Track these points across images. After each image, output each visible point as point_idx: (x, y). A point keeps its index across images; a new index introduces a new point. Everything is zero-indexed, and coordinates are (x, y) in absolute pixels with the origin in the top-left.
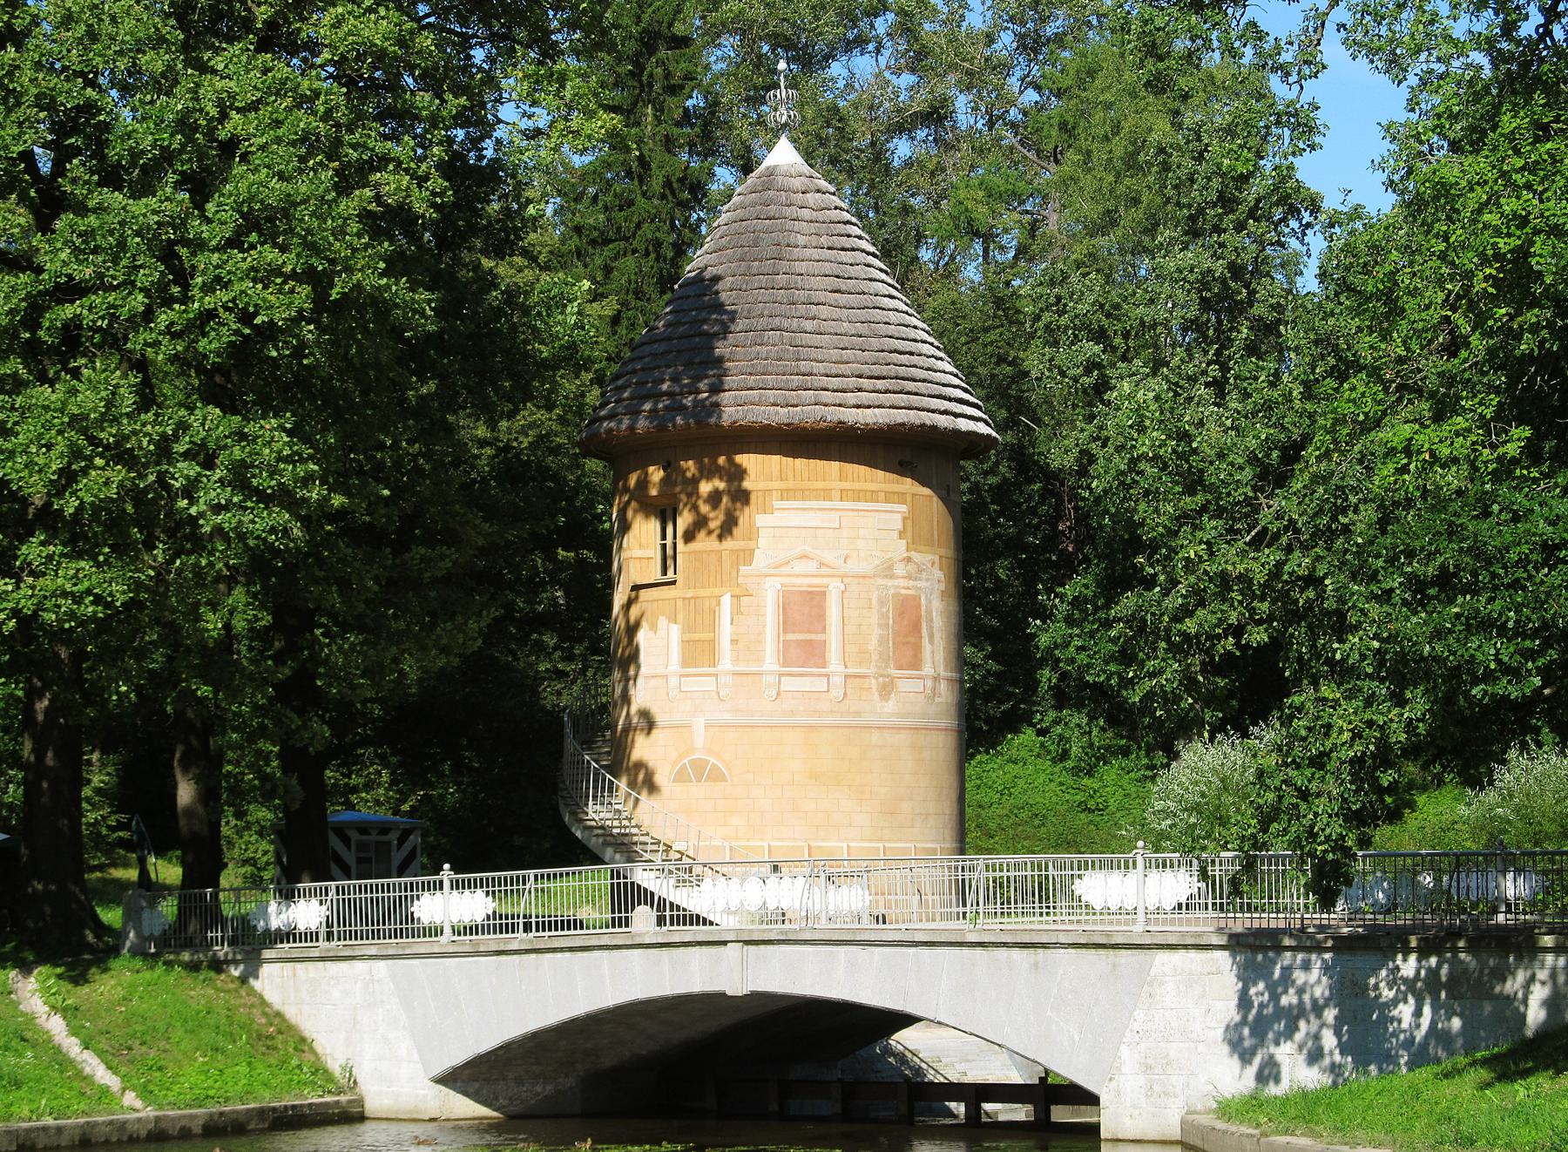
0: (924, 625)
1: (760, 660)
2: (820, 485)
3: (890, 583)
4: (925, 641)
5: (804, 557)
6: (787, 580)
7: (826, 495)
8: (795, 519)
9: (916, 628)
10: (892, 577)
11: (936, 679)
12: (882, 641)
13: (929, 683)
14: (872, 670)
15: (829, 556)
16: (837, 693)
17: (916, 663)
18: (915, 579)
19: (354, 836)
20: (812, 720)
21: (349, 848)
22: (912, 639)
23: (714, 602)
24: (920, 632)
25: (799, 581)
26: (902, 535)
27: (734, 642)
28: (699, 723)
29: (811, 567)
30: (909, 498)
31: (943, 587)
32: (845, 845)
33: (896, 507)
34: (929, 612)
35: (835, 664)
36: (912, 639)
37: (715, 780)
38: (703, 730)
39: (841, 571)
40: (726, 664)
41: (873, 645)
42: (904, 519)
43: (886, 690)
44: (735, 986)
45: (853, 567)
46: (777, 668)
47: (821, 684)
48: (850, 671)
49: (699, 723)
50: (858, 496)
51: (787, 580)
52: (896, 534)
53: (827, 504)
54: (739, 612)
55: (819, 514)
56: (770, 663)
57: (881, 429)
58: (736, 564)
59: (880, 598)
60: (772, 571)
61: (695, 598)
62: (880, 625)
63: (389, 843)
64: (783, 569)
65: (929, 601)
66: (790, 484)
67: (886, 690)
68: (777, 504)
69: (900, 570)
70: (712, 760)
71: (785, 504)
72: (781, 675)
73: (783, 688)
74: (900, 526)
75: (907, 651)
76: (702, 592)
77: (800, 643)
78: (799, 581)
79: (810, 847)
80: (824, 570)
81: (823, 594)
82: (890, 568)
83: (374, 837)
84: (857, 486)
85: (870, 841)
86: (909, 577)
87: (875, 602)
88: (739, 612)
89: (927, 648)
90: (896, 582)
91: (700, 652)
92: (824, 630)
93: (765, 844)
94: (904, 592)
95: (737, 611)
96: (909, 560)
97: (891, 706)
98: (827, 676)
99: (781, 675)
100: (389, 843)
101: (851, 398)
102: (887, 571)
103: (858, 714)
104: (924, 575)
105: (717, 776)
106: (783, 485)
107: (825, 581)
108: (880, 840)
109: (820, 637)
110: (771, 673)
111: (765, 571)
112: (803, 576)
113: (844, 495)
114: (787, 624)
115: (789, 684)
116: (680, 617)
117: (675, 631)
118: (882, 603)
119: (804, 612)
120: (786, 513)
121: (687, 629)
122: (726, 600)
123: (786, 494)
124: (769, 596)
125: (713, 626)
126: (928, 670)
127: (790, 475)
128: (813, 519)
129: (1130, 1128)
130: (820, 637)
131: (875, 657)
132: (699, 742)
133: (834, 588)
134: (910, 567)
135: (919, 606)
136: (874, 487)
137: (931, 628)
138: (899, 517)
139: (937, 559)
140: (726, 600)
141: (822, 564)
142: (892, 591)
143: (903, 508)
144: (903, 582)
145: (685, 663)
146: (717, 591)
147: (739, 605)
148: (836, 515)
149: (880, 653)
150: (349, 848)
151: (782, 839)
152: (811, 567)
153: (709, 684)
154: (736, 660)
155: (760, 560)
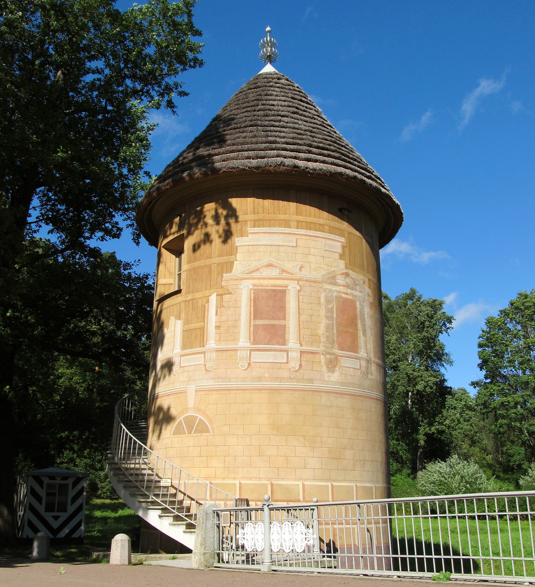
0: (359, 321)
1: (236, 340)
2: (282, 217)
3: (334, 288)
4: (360, 334)
6: (256, 282)
7: (287, 224)
8: (265, 239)
9: (353, 323)
10: (335, 284)
11: (368, 361)
12: (328, 328)
13: (364, 363)
14: (321, 348)
15: (288, 266)
16: (294, 364)
17: (354, 347)
19: (46, 481)
20: (276, 384)
21: (42, 487)
22: (351, 330)
23: (205, 300)
24: (356, 326)
25: (266, 282)
26: (342, 257)
27: (218, 327)
28: (191, 389)
29: (275, 273)
30: (346, 235)
31: (371, 300)
32: (300, 483)
33: (337, 238)
35: (292, 343)
36: (351, 330)
37: (201, 432)
38: (194, 393)
39: (298, 276)
40: (211, 344)
41: (321, 330)
42: (343, 247)
43: (332, 364)
45: (306, 274)
46: (248, 345)
47: (281, 358)
48: (305, 348)
49: (191, 389)
50: (309, 226)
51: (256, 282)
52: (337, 256)
53: (287, 230)
54: (222, 306)
55: (281, 236)
56: (243, 341)
57: (325, 175)
58: (220, 274)
59: (326, 297)
60: (246, 276)
61: (193, 300)
62: (327, 317)
63: (67, 485)
64: (254, 274)
65: (362, 307)
66: (261, 216)
67: (332, 364)
68: (250, 230)
69: (341, 280)
70: (200, 417)
71: (256, 230)
72: (251, 350)
73: (253, 360)
74: (340, 250)
76: (198, 295)
77: (265, 327)
78: (266, 282)
79: (272, 485)
80: (285, 275)
82: (334, 278)
83: (58, 481)
84: (309, 219)
85: (321, 480)
86: (347, 286)
87: (323, 300)
88: (222, 306)
89: (361, 339)
91: (194, 338)
92: (284, 318)
93: (237, 482)
94: (343, 295)
95: (220, 305)
97: (335, 376)
98: (287, 351)
99: (251, 350)
100: (67, 485)
101: (302, 155)
102: (332, 279)
103: (311, 380)
104: (358, 288)
105: (202, 429)
106: (256, 217)
107: (286, 282)
108: (328, 480)
109: (281, 322)
110: (243, 349)
111: (241, 276)
112: (269, 279)
113: (299, 225)
114: (257, 313)
115: (257, 357)
116: (183, 315)
117: (179, 323)
118: (328, 301)
119: (269, 305)
120: (257, 236)
121: (187, 322)
122: (213, 299)
123: (257, 223)
125: (203, 317)
126: (362, 353)
127: (261, 210)
128: (277, 240)
130: (281, 322)
131: (323, 339)
132: (191, 404)
133: (292, 288)
135: (355, 308)
136: (321, 221)
137: (364, 325)
138: (340, 244)
139: (367, 280)
140: (213, 299)
141: (283, 271)
142: (335, 294)
143: (343, 240)
144: (342, 289)
145: (184, 346)
146: (207, 293)
147: (222, 300)
148: (294, 238)
149: (327, 337)
150: (42, 487)
151: (250, 479)
152: (275, 273)
153: (199, 359)
154: (219, 341)
155: (238, 268)
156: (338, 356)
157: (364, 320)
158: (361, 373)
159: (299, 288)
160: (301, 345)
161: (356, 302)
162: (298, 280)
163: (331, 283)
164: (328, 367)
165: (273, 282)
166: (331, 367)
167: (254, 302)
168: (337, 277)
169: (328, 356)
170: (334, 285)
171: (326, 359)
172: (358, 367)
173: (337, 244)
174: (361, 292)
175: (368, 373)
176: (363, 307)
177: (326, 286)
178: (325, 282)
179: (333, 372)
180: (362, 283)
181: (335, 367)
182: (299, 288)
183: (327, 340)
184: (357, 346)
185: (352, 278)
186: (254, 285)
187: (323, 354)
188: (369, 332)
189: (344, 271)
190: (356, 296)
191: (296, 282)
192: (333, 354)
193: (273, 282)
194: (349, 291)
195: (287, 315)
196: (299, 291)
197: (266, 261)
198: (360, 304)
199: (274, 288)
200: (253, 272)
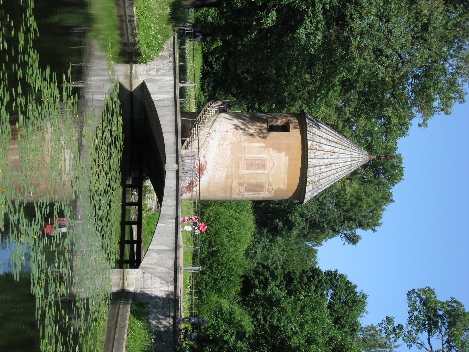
1: (248, 153)
3: (267, 185)
5: (274, 164)
10: (268, 185)
13: (242, 194)
17: (247, 190)
18: (268, 191)
25: (268, 163)
29: (271, 166)
31: (266, 197)
34: (260, 194)
43: (240, 184)
44: (167, 167)
67: (240, 184)
75: (251, 188)
80: (270, 169)
82: (271, 185)
90: (267, 186)
96: (273, 189)
112: (269, 164)
118: (262, 183)
124: (264, 155)
126: (245, 193)
129: (127, 276)
131: (249, 181)
133: (266, 172)
134: (271, 190)
141: (272, 169)
143: (285, 188)
165: (268, 165)
177: (267, 183)
188: (254, 196)
193: (268, 165)
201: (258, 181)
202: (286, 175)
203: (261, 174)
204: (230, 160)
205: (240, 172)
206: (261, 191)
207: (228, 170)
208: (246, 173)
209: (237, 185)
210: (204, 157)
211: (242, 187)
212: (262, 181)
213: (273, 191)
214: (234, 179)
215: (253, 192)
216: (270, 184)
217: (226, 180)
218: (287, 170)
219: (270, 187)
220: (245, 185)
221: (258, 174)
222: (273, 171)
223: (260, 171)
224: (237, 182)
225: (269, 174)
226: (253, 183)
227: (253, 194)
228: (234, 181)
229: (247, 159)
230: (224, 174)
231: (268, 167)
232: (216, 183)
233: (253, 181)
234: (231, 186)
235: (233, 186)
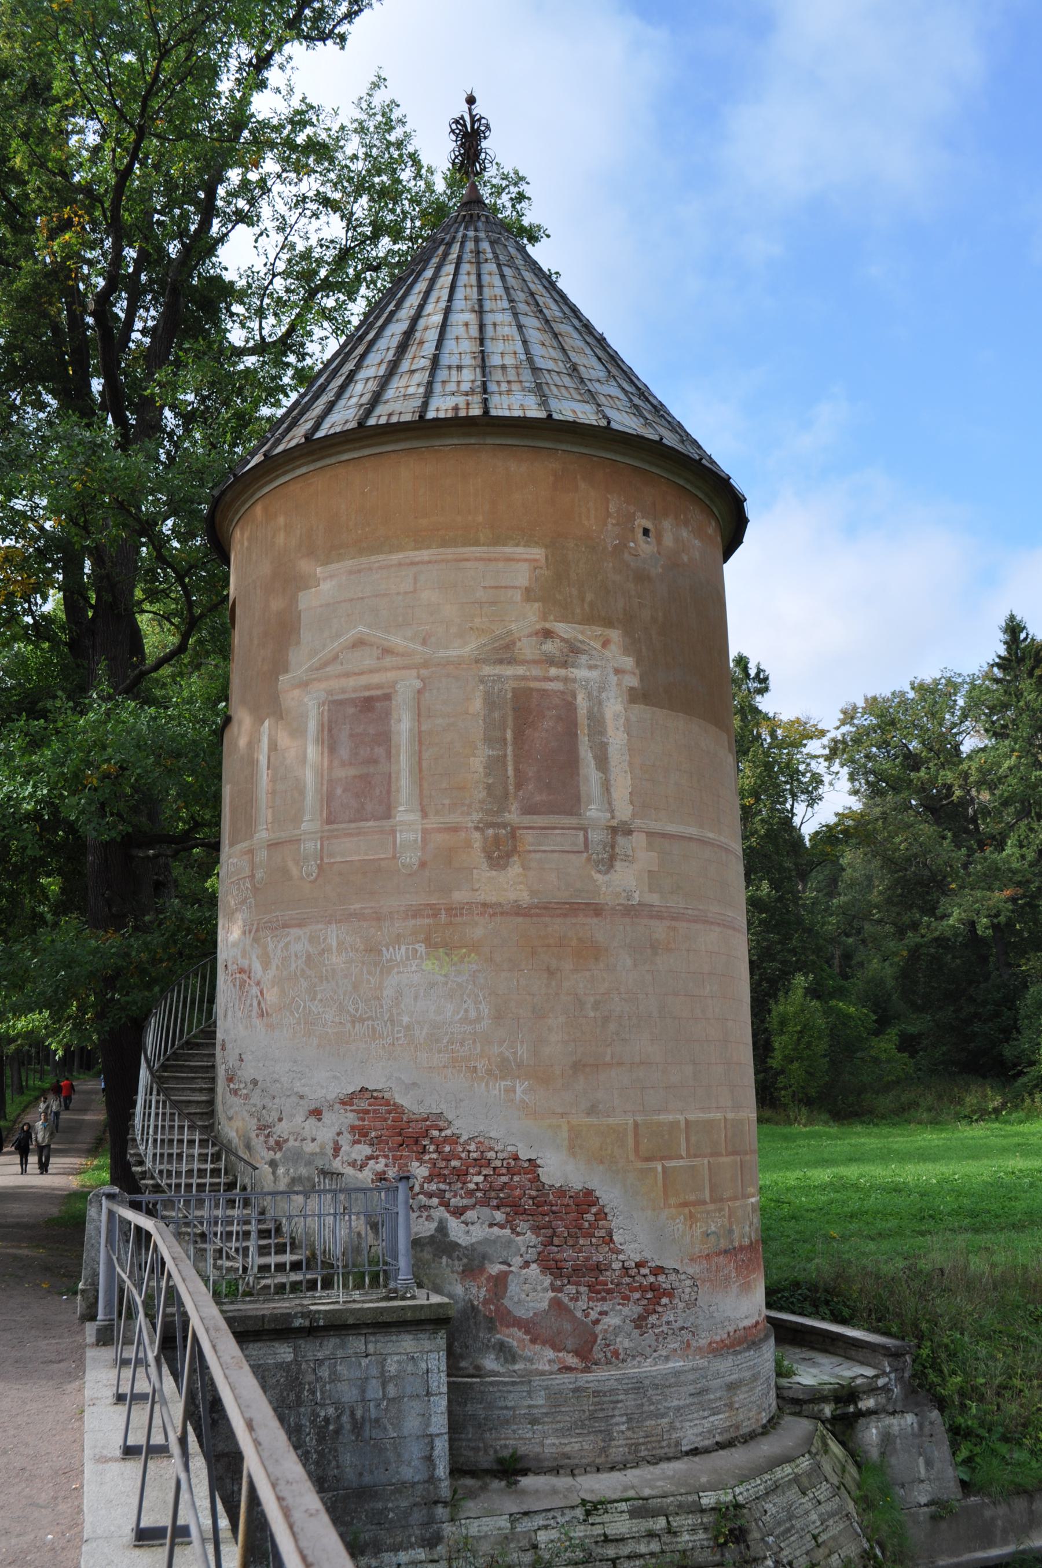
1: (297, 820)
3: (509, 671)
5: (359, 643)
6: (335, 684)
10: (512, 661)
13: (596, 836)
18: (565, 665)
25: (351, 682)
26: (529, 594)
29: (367, 659)
52: (518, 596)
62: (488, 740)
67: (502, 851)
80: (388, 661)
81: (388, 697)
82: (509, 646)
90: (520, 670)
96: (548, 634)
104: (583, 659)
107: (391, 675)
118: (491, 703)
126: (594, 812)
133: (407, 685)
134: (549, 647)
141: (387, 651)
143: (537, 553)
149: (489, 787)
156: (519, 828)
157: (603, 733)
158: (589, 859)
159: (418, 684)
160: (425, 815)
161: (575, 697)
162: (417, 667)
163: (501, 662)
164: (489, 858)
165: (364, 680)
166: (499, 857)
167: (330, 730)
168: (518, 644)
169: (490, 832)
170: (509, 663)
171: (485, 839)
172: (582, 848)
173: (522, 564)
174: (591, 667)
175: (612, 858)
176: (600, 703)
177: (487, 670)
178: (485, 661)
179: (504, 867)
180: (598, 646)
181: (508, 855)
182: (418, 684)
183: (489, 795)
184: (578, 798)
185: (563, 640)
186: (330, 693)
187: (477, 828)
189: (538, 627)
190: (574, 680)
191: (414, 672)
192: (504, 825)
194: (553, 671)
195: (393, 751)
196: (419, 692)
197: (352, 634)
198: (590, 695)
199: (367, 694)
200: (326, 664)
201: (477, 730)
202: (425, 554)
203: (420, 714)
204: (333, 934)
205: (411, 858)
206: (571, 707)
207: (398, 940)
208: (414, 817)
209: (515, 870)
210: (316, 1113)
211: (528, 838)
212: (477, 705)
213: (562, 628)
214: (460, 896)
215: (571, 764)
216: (504, 652)
217: (474, 947)
218: (396, 557)
219: (527, 648)
220: (513, 816)
221: (420, 738)
222: (397, 641)
223: (403, 725)
224: (484, 873)
225: (425, 665)
226: (495, 765)
227: (602, 762)
228: (482, 897)
229: (329, 822)
230: (428, 965)
231: (376, 679)
232: (498, 1017)
233: (477, 763)
234: (518, 911)
235: (524, 897)
